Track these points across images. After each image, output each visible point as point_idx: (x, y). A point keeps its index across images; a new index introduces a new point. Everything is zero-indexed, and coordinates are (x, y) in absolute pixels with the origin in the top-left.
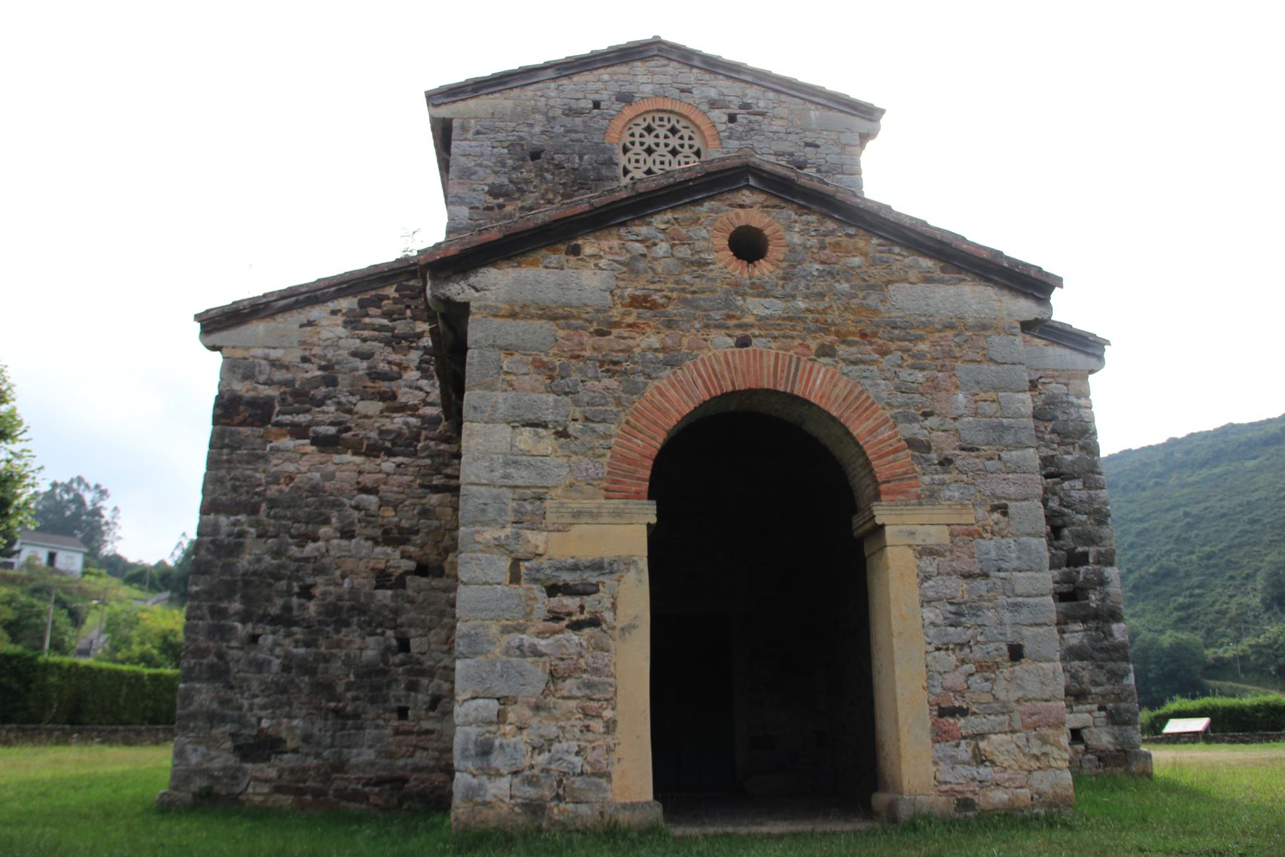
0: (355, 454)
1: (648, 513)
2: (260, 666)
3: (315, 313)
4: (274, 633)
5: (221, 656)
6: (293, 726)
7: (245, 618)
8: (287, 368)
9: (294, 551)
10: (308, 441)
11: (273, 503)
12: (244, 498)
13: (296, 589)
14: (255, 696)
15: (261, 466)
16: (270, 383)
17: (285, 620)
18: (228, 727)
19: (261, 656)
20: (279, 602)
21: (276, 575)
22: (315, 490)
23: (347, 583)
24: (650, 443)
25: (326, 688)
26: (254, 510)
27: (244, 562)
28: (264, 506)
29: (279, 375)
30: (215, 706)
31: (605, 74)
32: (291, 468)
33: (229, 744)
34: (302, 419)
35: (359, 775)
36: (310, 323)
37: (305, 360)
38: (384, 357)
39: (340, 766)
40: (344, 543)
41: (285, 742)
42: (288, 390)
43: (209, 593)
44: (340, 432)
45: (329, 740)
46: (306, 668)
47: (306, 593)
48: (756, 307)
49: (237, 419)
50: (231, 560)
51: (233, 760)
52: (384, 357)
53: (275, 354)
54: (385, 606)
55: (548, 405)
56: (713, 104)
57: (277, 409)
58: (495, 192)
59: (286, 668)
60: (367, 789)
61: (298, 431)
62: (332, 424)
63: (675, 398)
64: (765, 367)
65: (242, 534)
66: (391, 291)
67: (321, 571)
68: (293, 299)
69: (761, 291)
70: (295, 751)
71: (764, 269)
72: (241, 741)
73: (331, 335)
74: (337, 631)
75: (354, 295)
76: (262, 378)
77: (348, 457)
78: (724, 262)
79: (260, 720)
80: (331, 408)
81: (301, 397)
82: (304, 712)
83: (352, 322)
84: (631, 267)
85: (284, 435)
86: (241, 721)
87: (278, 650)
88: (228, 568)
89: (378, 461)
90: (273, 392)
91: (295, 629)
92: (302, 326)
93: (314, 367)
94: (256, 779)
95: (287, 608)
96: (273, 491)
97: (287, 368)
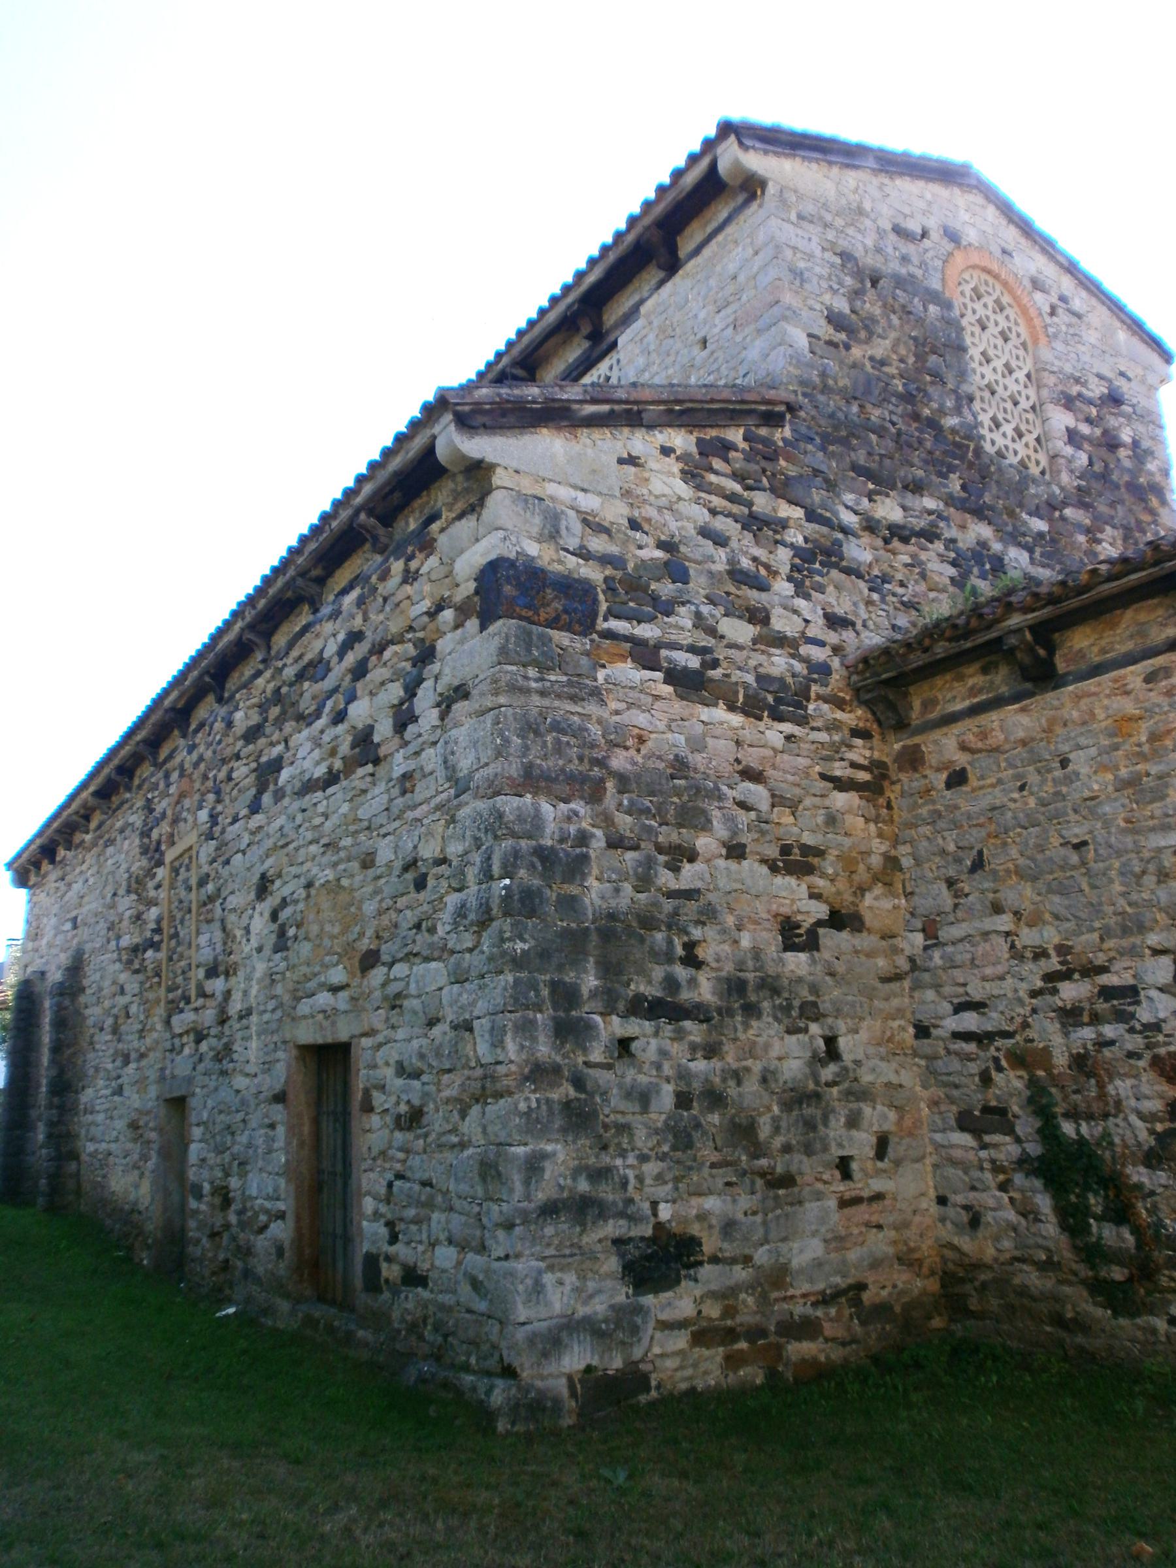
0: (731, 708)
2: (644, 1098)
3: (640, 442)
4: (656, 1034)
5: (578, 1082)
6: (708, 1207)
7: (610, 1002)
8: (607, 531)
9: (665, 878)
10: (659, 675)
11: (623, 781)
12: (574, 766)
13: (680, 951)
14: (644, 1158)
15: (592, 708)
16: (583, 554)
17: (665, 1009)
18: (613, 1228)
19: (643, 1079)
20: (658, 973)
21: (648, 922)
22: (680, 766)
23: (746, 941)
25: (743, 1132)
26: (595, 795)
27: (595, 892)
28: (610, 785)
29: (598, 544)
30: (583, 1186)
32: (641, 719)
33: (612, 1264)
34: (647, 631)
35: (806, 1287)
36: (632, 460)
37: (634, 525)
38: (747, 549)
39: (779, 1276)
40: (733, 865)
41: (700, 1244)
42: (619, 574)
43: (544, 954)
44: (704, 664)
45: (761, 1232)
46: (715, 1099)
47: (692, 960)
49: (543, 616)
50: (573, 889)
51: (622, 1294)
52: (747, 549)
53: (589, 502)
54: (800, 980)
57: (604, 607)
59: (683, 1100)
60: (819, 1313)
61: (645, 655)
62: (692, 649)
65: (583, 839)
66: (736, 435)
67: (708, 915)
68: (605, 408)
70: (715, 1260)
72: (633, 1252)
73: (667, 491)
74: (747, 1026)
75: (690, 426)
76: (573, 543)
77: (720, 713)
79: (654, 1205)
80: (684, 617)
81: (634, 591)
82: (720, 1183)
83: (693, 474)
85: (623, 658)
86: (626, 1212)
87: (667, 1070)
88: (569, 904)
89: (761, 725)
90: (593, 573)
91: (687, 1024)
92: (621, 461)
93: (651, 541)
94: (665, 1326)
95: (671, 984)
96: (619, 761)
97: (607, 531)
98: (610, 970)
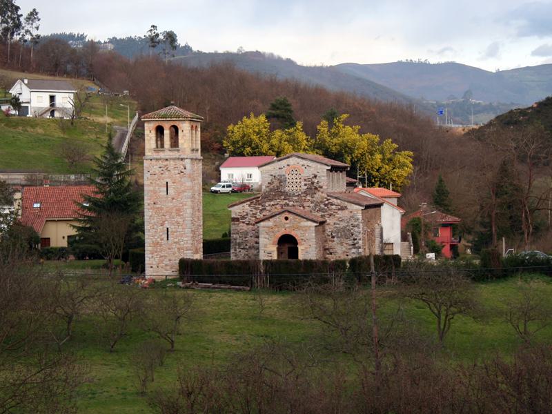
1: (277, 246)
3: (244, 204)
24: (277, 240)
27: (238, 241)
31: (285, 161)
38: (254, 211)
47: (246, 245)
48: (287, 226)
52: (254, 211)
55: (267, 236)
56: (303, 165)
58: (269, 183)
61: (244, 222)
63: (279, 235)
64: (288, 232)
66: (254, 201)
69: (287, 223)
71: (288, 221)
78: (284, 221)
81: (243, 217)
83: (249, 206)
84: (274, 222)
98: (239, 246)
